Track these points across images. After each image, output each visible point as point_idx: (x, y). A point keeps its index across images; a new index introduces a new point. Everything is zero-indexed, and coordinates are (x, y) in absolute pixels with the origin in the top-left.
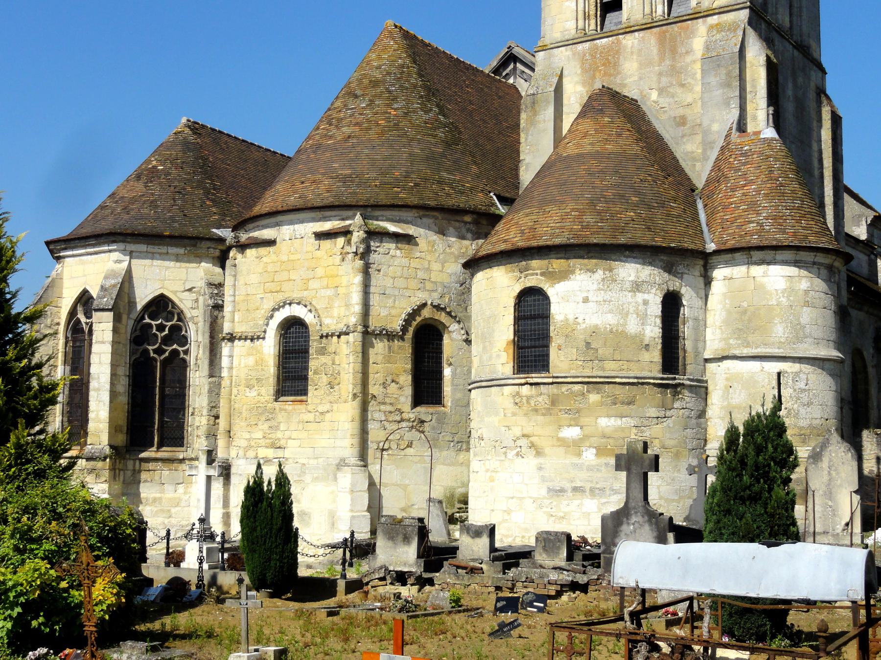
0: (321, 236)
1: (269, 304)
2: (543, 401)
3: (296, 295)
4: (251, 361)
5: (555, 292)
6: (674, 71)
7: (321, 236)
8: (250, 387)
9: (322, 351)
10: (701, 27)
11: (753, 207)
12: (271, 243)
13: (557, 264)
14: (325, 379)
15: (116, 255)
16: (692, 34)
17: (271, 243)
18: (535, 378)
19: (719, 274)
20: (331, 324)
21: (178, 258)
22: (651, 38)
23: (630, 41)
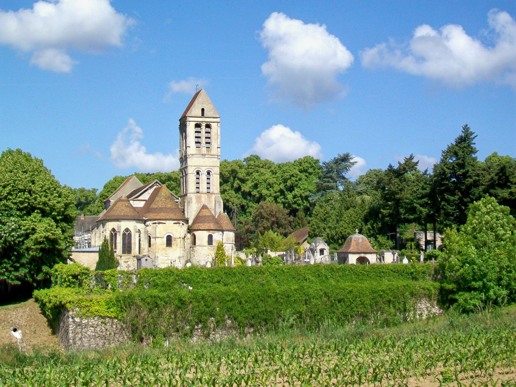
0: (174, 223)
1: (165, 233)
2: (212, 249)
3: (170, 232)
4: (162, 241)
5: (213, 235)
6: (210, 201)
7: (174, 223)
8: (161, 245)
9: (175, 240)
10: (214, 196)
11: (227, 224)
12: (165, 223)
13: (214, 231)
14: (175, 245)
15: (135, 223)
16: (212, 196)
17: (165, 223)
18: (211, 246)
19: (225, 232)
20: (177, 236)
21: (140, 223)
22: (206, 196)
23: (203, 195)
